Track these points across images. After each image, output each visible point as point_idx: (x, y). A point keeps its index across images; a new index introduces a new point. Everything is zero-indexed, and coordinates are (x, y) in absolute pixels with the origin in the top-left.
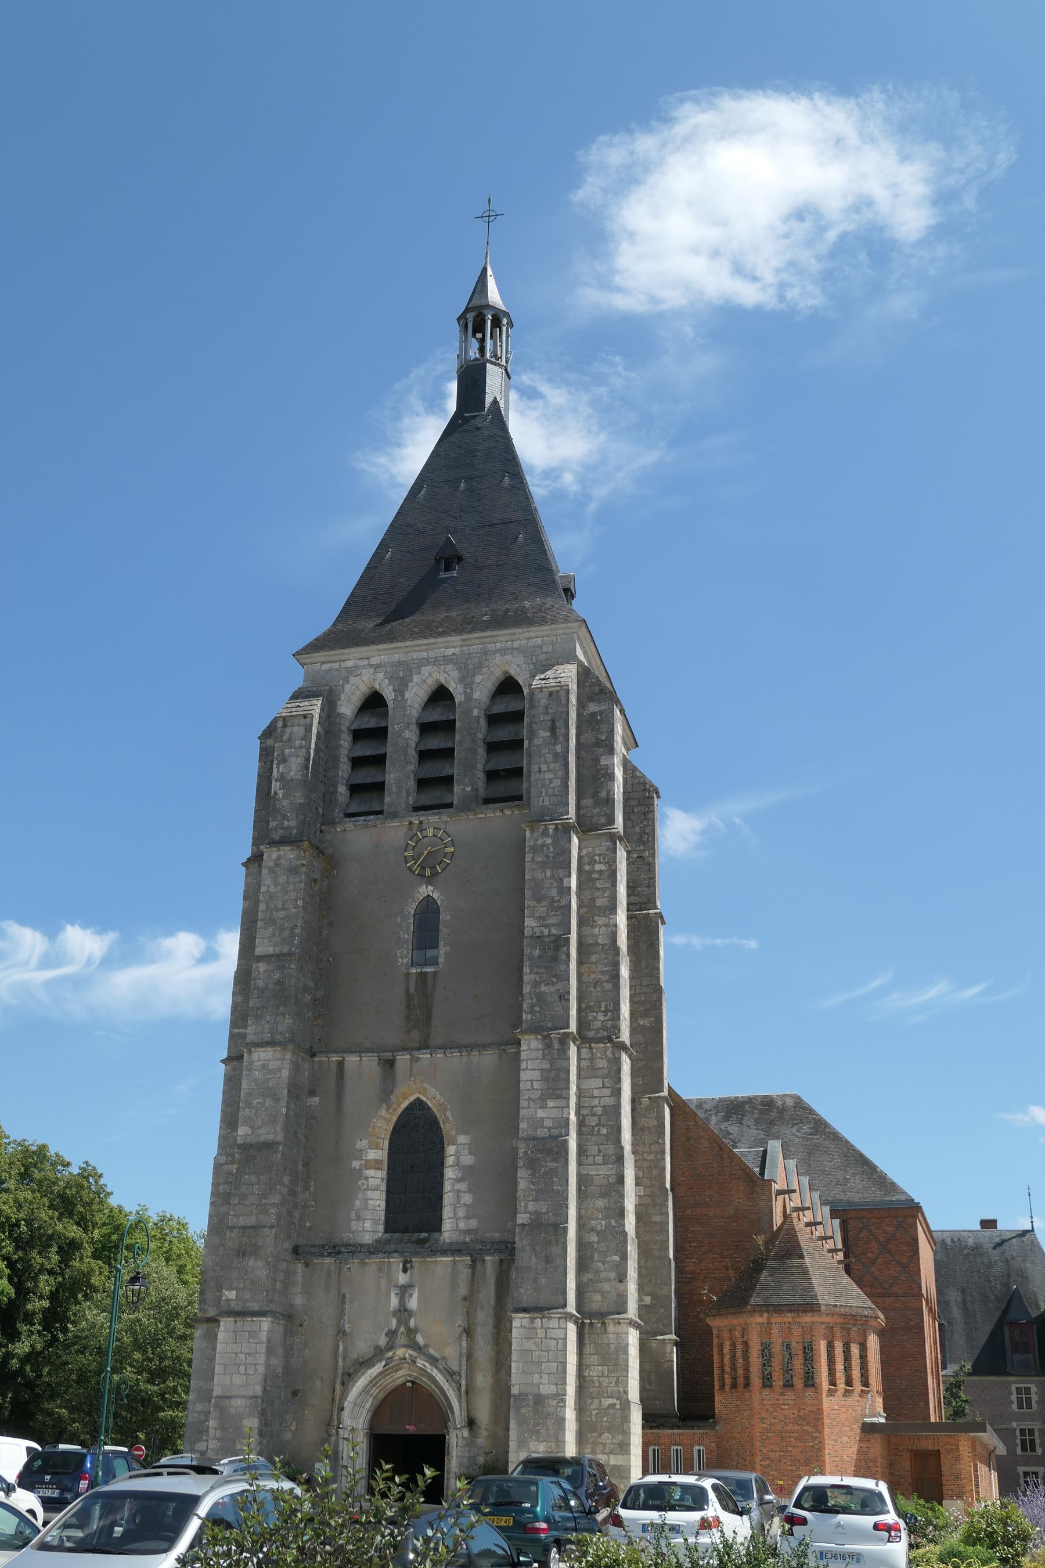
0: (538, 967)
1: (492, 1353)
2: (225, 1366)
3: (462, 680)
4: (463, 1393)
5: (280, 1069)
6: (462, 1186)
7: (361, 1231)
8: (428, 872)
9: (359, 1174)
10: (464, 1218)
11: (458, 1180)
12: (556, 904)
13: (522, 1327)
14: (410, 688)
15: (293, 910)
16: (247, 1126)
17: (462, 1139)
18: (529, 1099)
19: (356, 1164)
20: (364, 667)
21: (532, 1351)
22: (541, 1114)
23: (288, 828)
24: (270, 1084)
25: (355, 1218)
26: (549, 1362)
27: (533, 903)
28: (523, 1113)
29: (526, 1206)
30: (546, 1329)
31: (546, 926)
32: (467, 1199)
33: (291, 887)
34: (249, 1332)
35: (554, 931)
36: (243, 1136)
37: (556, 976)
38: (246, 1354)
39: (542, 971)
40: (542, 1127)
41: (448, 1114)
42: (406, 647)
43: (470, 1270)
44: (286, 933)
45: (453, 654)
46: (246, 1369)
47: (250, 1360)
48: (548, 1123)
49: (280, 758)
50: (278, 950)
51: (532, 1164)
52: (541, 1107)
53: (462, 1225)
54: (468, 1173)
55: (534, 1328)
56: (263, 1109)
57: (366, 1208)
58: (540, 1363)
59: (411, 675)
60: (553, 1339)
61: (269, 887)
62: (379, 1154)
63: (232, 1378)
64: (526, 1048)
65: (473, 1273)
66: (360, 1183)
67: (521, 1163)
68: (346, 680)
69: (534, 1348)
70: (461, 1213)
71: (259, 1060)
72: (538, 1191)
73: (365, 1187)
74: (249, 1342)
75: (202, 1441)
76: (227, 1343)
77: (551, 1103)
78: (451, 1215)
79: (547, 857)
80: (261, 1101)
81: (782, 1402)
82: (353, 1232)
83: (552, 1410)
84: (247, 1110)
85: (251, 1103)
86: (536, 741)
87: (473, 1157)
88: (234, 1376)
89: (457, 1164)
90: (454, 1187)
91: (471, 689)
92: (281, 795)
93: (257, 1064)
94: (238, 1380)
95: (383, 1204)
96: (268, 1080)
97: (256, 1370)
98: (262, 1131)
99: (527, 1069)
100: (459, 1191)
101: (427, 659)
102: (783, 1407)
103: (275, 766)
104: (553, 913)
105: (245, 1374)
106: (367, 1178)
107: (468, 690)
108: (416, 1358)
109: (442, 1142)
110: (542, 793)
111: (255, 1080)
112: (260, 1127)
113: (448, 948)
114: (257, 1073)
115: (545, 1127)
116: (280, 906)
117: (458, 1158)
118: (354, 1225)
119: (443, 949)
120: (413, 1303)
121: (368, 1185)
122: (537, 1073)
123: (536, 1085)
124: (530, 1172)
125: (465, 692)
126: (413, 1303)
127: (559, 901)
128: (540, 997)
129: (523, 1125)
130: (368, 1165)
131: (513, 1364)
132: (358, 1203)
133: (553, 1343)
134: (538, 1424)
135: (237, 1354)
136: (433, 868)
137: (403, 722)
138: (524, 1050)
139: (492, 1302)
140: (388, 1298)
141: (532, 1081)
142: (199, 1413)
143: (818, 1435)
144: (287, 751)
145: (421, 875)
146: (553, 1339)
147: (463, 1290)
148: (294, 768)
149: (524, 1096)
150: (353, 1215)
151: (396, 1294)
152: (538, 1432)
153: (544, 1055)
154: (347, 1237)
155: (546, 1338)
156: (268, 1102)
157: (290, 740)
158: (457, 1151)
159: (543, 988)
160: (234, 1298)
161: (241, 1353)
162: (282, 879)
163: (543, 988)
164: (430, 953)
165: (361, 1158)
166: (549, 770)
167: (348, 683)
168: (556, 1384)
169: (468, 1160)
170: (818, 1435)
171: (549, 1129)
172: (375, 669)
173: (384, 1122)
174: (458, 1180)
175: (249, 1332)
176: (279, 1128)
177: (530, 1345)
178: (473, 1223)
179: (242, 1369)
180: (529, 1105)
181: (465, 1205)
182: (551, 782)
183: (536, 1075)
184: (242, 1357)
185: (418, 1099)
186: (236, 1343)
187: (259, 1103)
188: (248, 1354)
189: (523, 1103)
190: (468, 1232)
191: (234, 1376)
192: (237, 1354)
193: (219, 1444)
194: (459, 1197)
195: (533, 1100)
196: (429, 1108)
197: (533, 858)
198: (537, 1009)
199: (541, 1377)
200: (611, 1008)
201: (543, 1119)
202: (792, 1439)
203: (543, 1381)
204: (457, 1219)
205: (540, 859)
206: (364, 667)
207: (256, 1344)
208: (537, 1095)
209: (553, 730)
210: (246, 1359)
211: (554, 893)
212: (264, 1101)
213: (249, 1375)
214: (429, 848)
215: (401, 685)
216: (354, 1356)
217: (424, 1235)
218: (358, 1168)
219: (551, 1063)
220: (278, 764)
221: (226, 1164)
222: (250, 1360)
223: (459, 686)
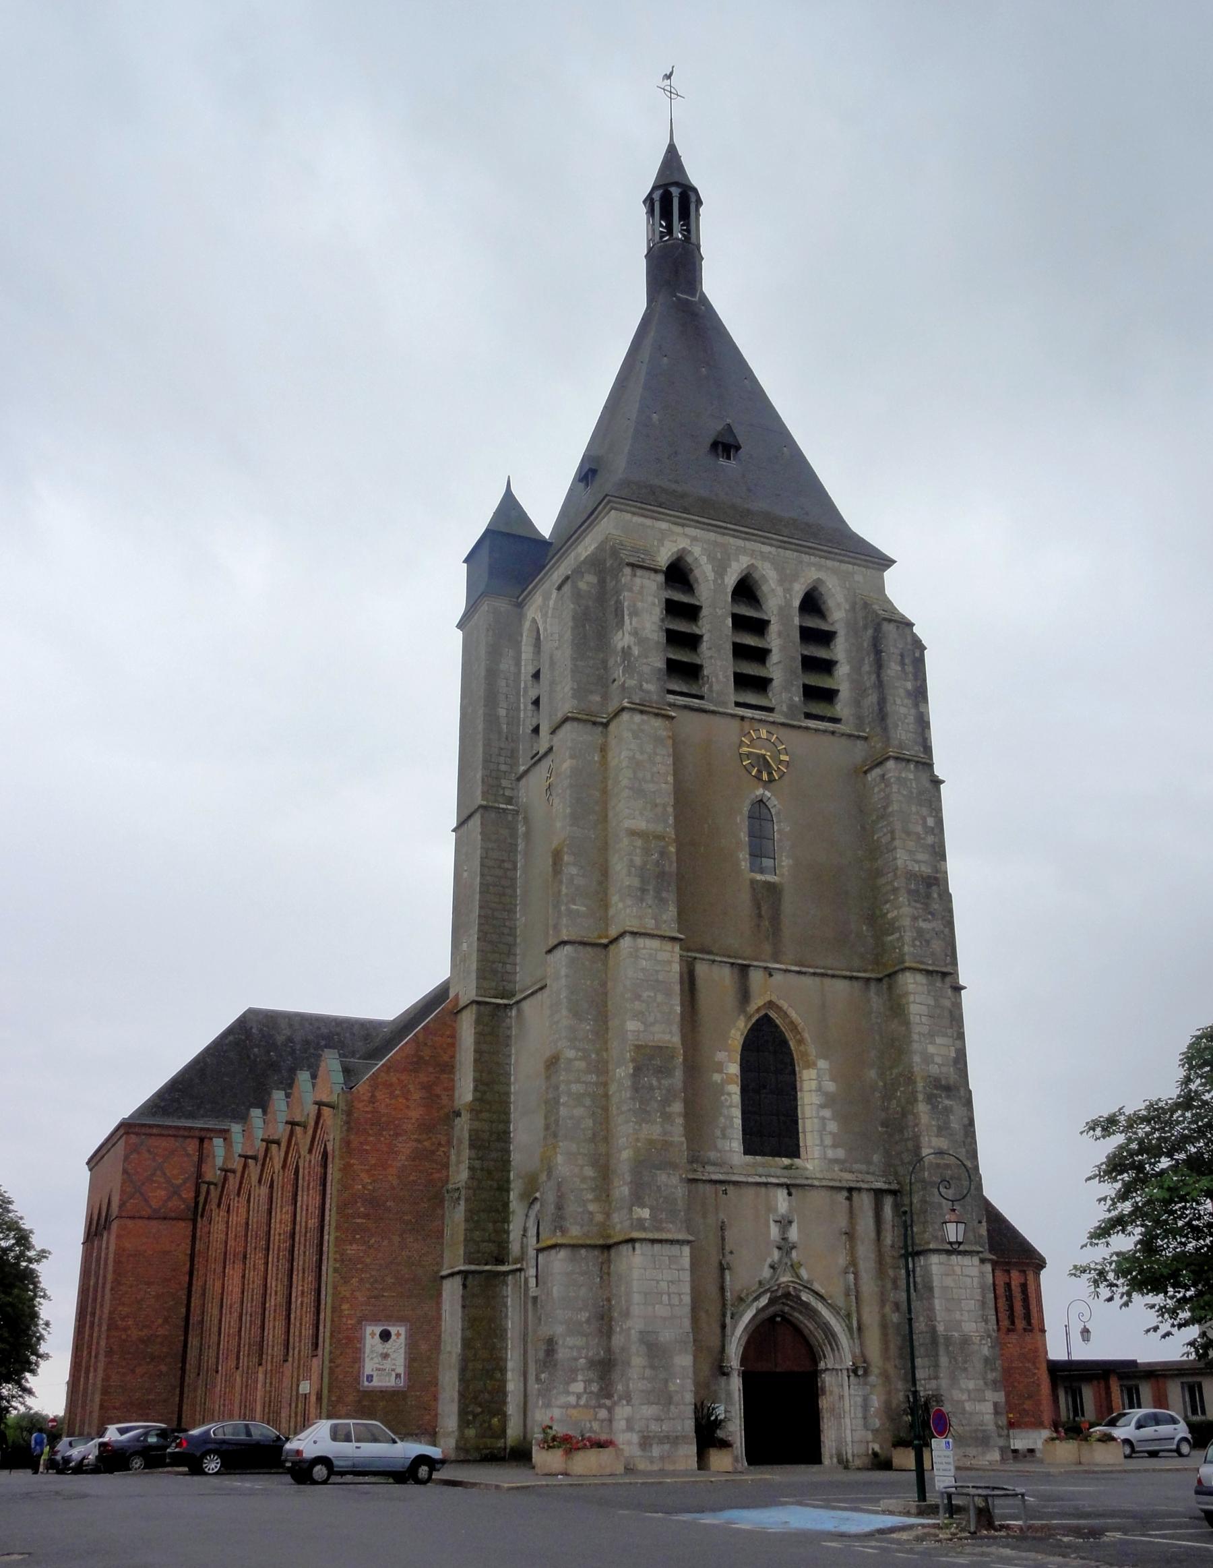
0: (916, 901)
1: (876, 1289)
2: (646, 1294)
3: (781, 582)
4: (855, 1329)
5: (669, 962)
6: (827, 1113)
7: (728, 1151)
8: (765, 776)
9: (720, 1090)
10: (831, 1147)
11: (823, 1106)
12: (922, 841)
13: (940, 1264)
14: (729, 574)
15: (663, 785)
16: (638, 1020)
17: (822, 1064)
18: (919, 1033)
19: (717, 1077)
20: (678, 534)
21: (952, 1288)
22: (931, 1049)
23: (648, 692)
24: (661, 978)
25: (721, 1136)
26: (967, 1299)
27: (904, 836)
28: (915, 1046)
29: (930, 1141)
30: (962, 1266)
31: (917, 862)
32: (833, 1126)
33: (658, 759)
34: (669, 1257)
35: (923, 869)
36: (634, 1031)
37: (930, 913)
38: (668, 1282)
39: (918, 905)
40: (933, 1062)
41: (806, 1035)
42: (726, 528)
43: (847, 1202)
44: (659, 810)
45: (770, 553)
46: (669, 1299)
47: (673, 1289)
48: (938, 1060)
49: (632, 609)
50: (652, 827)
51: (930, 1099)
52: (931, 1043)
53: (830, 1154)
54: (829, 1101)
55: (951, 1265)
56: (655, 1005)
57: (732, 1126)
58: (960, 1300)
59: (729, 559)
60: (967, 1276)
61: (634, 754)
62: (734, 1069)
63: (654, 1308)
64: (912, 981)
65: (851, 1206)
66: (723, 1098)
67: (920, 1097)
68: (661, 541)
69: (952, 1285)
70: (828, 1141)
71: (644, 948)
72: (940, 1128)
73: (728, 1104)
74: (670, 1268)
75: (577, 1381)
76: (645, 1269)
77: (939, 1040)
78: (818, 1142)
79: (912, 793)
80: (653, 995)
81: (1007, 1341)
82: (720, 1152)
83: (975, 1347)
84: (636, 1003)
85: (640, 996)
86: (889, 671)
87: (834, 1084)
88: (657, 1306)
89: (819, 1089)
90: (818, 1114)
91: (791, 595)
92: (637, 653)
93: (644, 951)
94: (661, 1311)
95: (740, 1122)
96: (657, 972)
97: (681, 1300)
98: (656, 1028)
99: (914, 1002)
100: (823, 1119)
101: (744, 548)
102: (1009, 1345)
103: (626, 617)
104: (920, 850)
105: (670, 1305)
106: (729, 1094)
107: (788, 595)
108: (800, 1291)
109: (793, 1065)
110: (898, 726)
111: (643, 970)
112: (653, 1024)
113: (791, 862)
114: (644, 963)
115: (937, 1064)
116: (649, 777)
117: (819, 1083)
118: (720, 1143)
119: (785, 862)
120: (793, 1234)
121: (731, 1102)
122: (923, 1007)
123: (924, 1019)
124: (929, 1107)
125: (785, 598)
126: (793, 1234)
127: (924, 839)
128: (920, 932)
129: (917, 1059)
130: (729, 1080)
131: (937, 1302)
132: (722, 1120)
133: (969, 1280)
134: (965, 1362)
135: (658, 1282)
136: (770, 774)
137: (724, 608)
138: (910, 983)
139: (873, 1235)
140: (769, 1227)
141: (920, 1015)
142: (571, 1348)
143: (1036, 1371)
144: (639, 604)
145: (758, 778)
146: (967, 1276)
147: (843, 1223)
148: (648, 625)
149: (916, 1029)
150: (718, 1133)
151: (776, 1222)
152: (965, 1370)
153: (929, 992)
154: (712, 1155)
155: (962, 1275)
156: (660, 998)
157: (641, 593)
158: (819, 1075)
159: (922, 924)
160: (648, 1216)
161: (663, 1280)
162: (649, 748)
163: (922, 924)
164: (767, 862)
165: (720, 1071)
166: (902, 705)
167: (663, 545)
168: (976, 1322)
169: (830, 1086)
170: (1036, 1371)
171: (940, 1066)
172: (691, 541)
173: (737, 1034)
174: (823, 1106)
175: (669, 1257)
176: (675, 1029)
177: (949, 1282)
178: (840, 1153)
179: (665, 1298)
180: (920, 1039)
181: (830, 1133)
182: (906, 718)
183: (923, 1010)
184: (664, 1285)
185: (766, 1015)
186: (655, 1268)
187: (649, 996)
188: (672, 1282)
189: (915, 1037)
190: (836, 1161)
191: (657, 1306)
192: (658, 1282)
193: (649, 1385)
194: (824, 1126)
195: (924, 1035)
196: (777, 1026)
197: (899, 792)
198: (918, 943)
199: (962, 1315)
200: (949, 953)
201: (933, 1055)
202: (1017, 1376)
203: (963, 1318)
204: (825, 1147)
205: (905, 793)
206: (678, 534)
207: (678, 1270)
208: (925, 1029)
209: (903, 664)
210: (669, 1287)
211: (919, 829)
212: (655, 995)
213: (674, 1305)
214: (769, 754)
215: (721, 571)
216: (738, 1287)
217: (786, 1161)
218: (719, 1081)
219: (936, 1000)
220: (630, 615)
221: (576, 1059)
222: (673, 1289)
223: (778, 588)
